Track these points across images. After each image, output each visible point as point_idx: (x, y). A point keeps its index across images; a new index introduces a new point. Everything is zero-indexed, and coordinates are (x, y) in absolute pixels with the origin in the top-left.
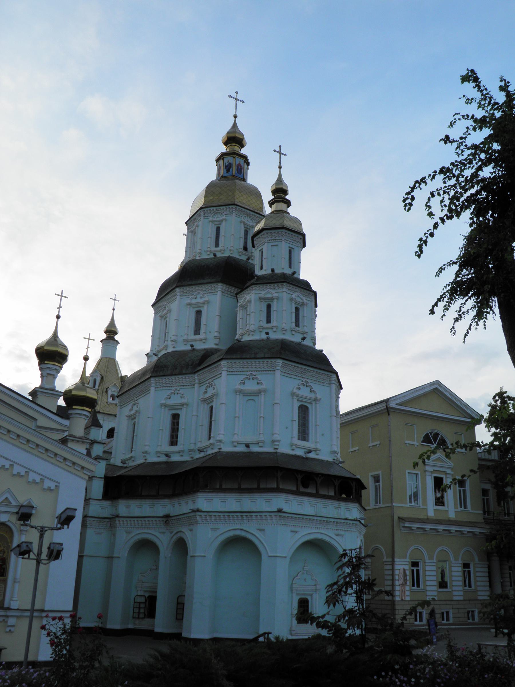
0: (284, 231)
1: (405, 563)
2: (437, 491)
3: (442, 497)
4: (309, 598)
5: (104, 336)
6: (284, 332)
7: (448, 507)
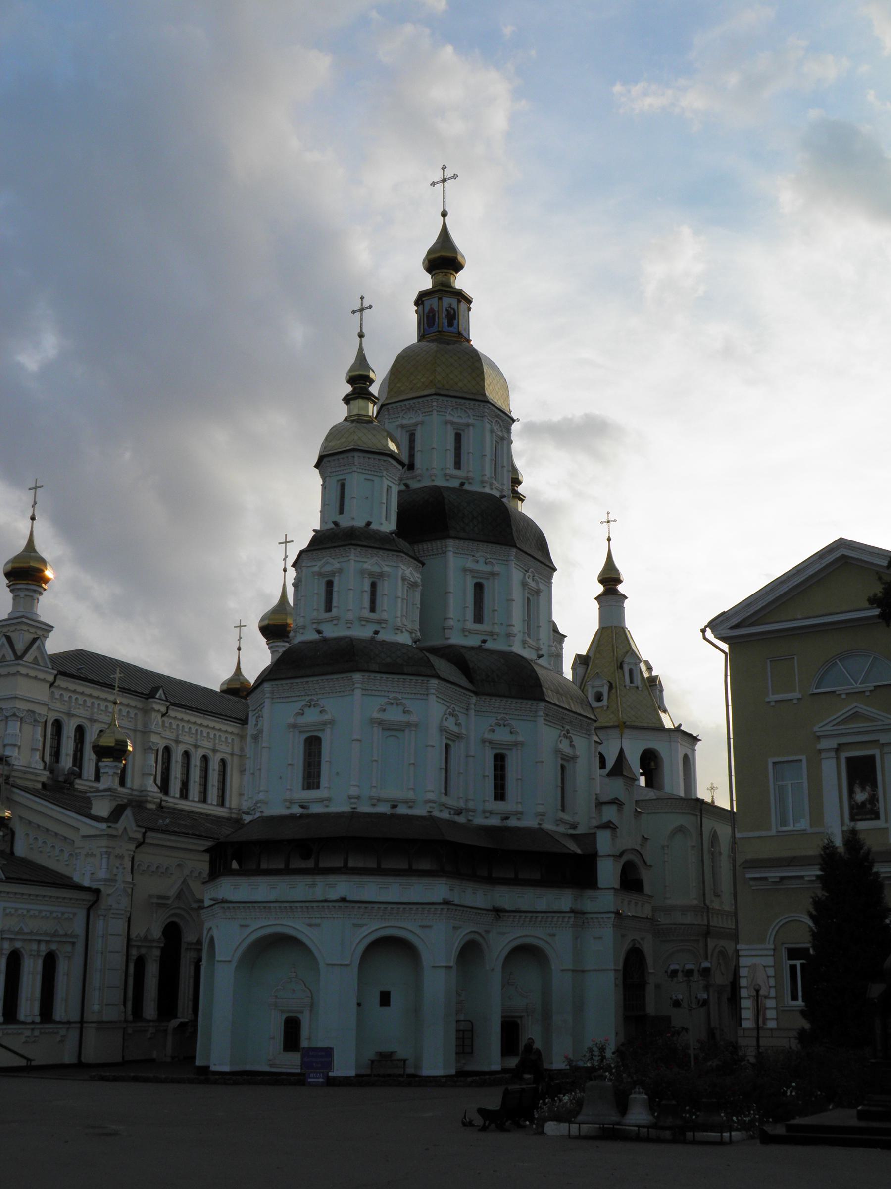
0: (356, 454)
1: (765, 953)
2: (857, 789)
3: (873, 799)
4: (519, 1021)
5: (600, 589)
6: (349, 625)
7: (886, 821)
